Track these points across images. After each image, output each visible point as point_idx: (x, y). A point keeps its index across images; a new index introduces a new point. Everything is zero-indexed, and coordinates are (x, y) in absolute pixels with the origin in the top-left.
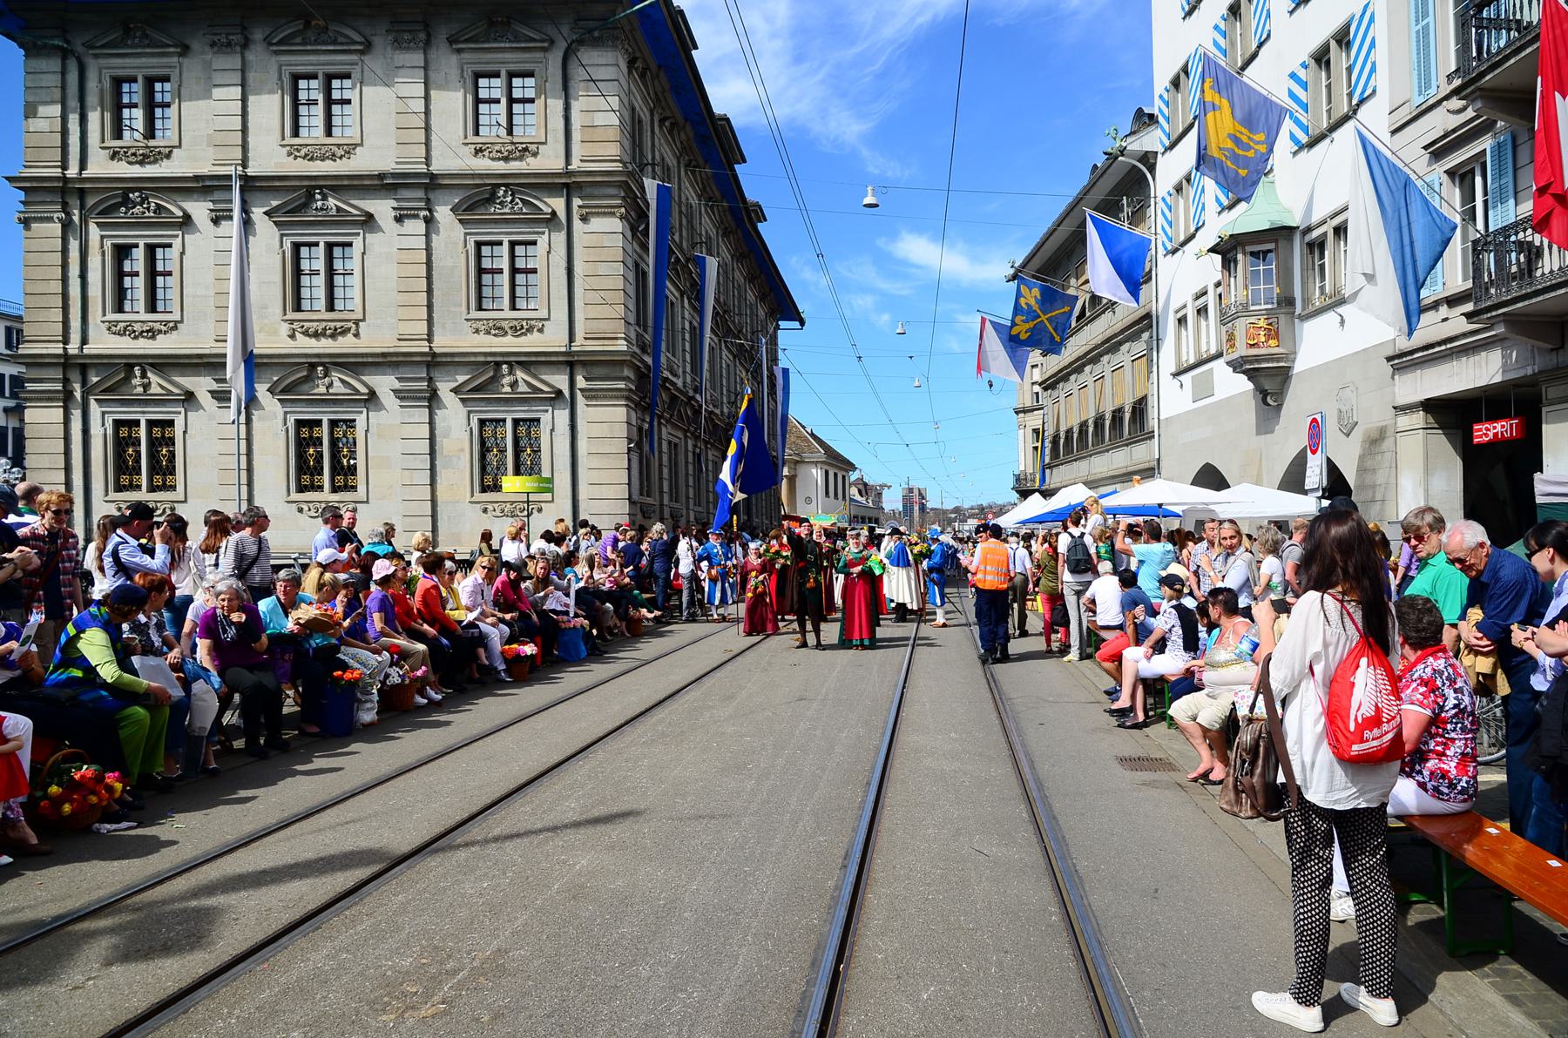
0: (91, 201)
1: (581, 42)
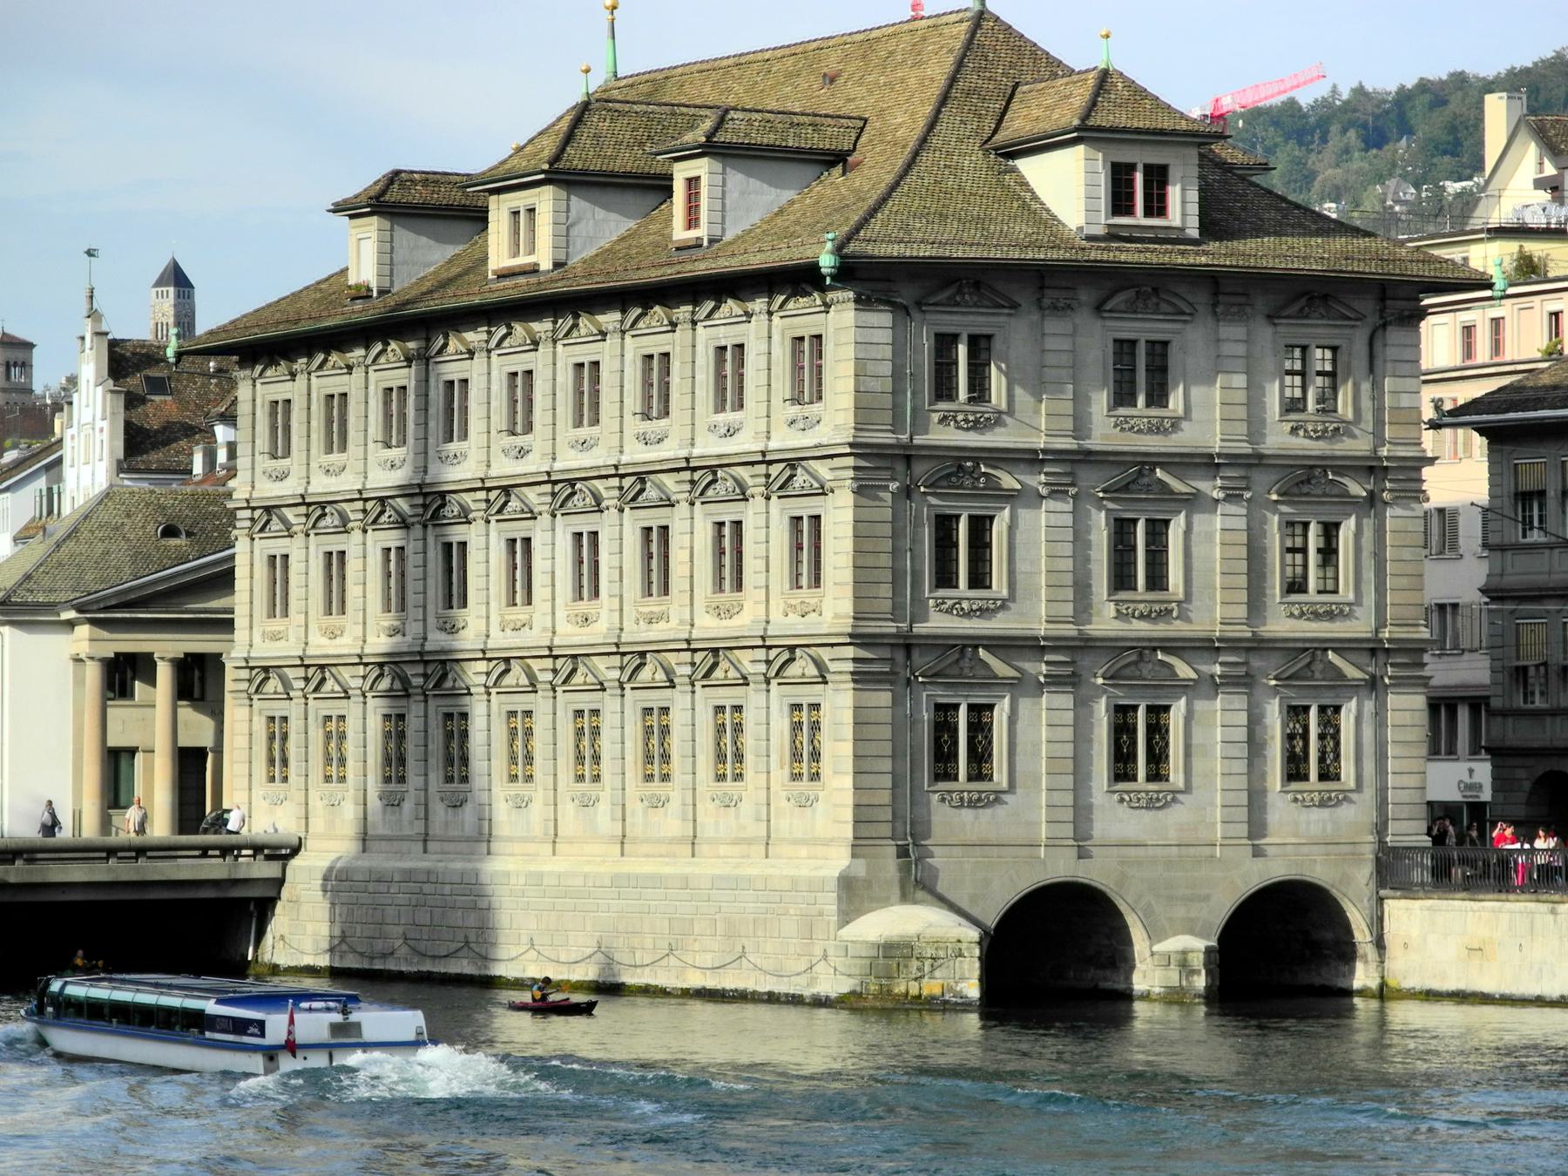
0: (920, 468)
1: (1384, 326)
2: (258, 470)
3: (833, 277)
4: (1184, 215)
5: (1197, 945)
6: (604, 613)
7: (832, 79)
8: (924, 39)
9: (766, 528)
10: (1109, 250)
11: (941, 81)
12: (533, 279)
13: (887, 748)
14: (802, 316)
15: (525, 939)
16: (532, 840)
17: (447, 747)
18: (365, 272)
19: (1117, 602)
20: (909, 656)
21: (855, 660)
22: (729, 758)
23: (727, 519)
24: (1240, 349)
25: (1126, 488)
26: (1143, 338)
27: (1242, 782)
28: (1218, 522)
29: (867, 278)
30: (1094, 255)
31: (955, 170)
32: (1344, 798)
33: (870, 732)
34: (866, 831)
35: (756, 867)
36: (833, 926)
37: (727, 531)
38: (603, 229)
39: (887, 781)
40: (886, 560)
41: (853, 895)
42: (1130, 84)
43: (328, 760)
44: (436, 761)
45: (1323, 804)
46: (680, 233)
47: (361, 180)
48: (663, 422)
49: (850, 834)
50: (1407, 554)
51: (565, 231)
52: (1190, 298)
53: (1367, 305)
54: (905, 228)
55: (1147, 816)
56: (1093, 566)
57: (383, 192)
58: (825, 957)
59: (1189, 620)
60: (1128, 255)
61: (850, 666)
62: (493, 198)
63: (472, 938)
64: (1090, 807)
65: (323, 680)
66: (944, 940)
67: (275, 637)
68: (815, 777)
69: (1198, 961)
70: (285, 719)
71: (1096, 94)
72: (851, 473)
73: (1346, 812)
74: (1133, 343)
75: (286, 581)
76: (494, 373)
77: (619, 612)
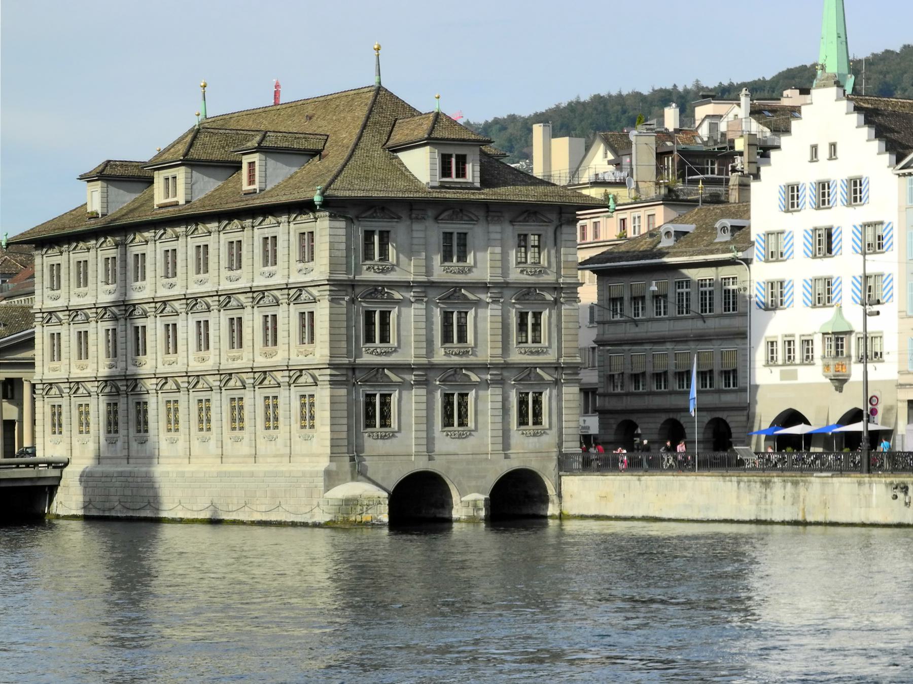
0: (358, 290)
1: (561, 225)
2: (45, 296)
3: (320, 206)
4: (473, 177)
5: (481, 498)
6: (212, 356)
7: (310, 118)
8: (353, 100)
9: (288, 318)
10: (441, 192)
11: (363, 119)
12: (176, 209)
13: (345, 414)
14: (304, 223)
15: (177, 501)
16: (179, 457)
17: (138, 417)
18: (95, 205)
19: (445, 348)
20: (354, 373)
21: (331, 375)
22: (271, 419)
23: (269, 314)
24: (498, 236)
25: (449, 298)
26: (456, 231)
27: (500, 426)
28: (489, 312)
29: (335, 206)
30: (435, 195)
31: (371, 157)
32: (544, 432)
33: (337, 407)
34: (336, 450)
35: (285, 467)
36: (322, 492)
37: (269, 319)
38: (207, 186)
39: (345, 428)
40: (344, 331)
41: (331, 478)
42: (449, 119)
43: (81, 424)
44: (133, 423)
45: (535, 435)
46: (246, 187)
47: (93, 164)
48: (239, 271)
49: (329, 451)
50: (571, 325)
51: (190, 187)
52: (476, 213)
53: (554, 216)
54: (351, 183)
55: (458, 442)
56: (434, 332)
57: (103, 170)
58: (318, 505)
59: (476, 356)
60: (450, 195)
61: (328, 378)
62: (156, 172)
63: (152, 501)
64: (433, 438)
65: (78, 388)
66: (373, 498)
67: (55, 370)
68: (312, 427)
69: (481, 504)
70: (60, 406)
71: (434, 124)
72: (328, 293)
73: (545, 439)
74: (451, 233)
75: (60, 345)
76: (158, 251)
77: (219, 355)
